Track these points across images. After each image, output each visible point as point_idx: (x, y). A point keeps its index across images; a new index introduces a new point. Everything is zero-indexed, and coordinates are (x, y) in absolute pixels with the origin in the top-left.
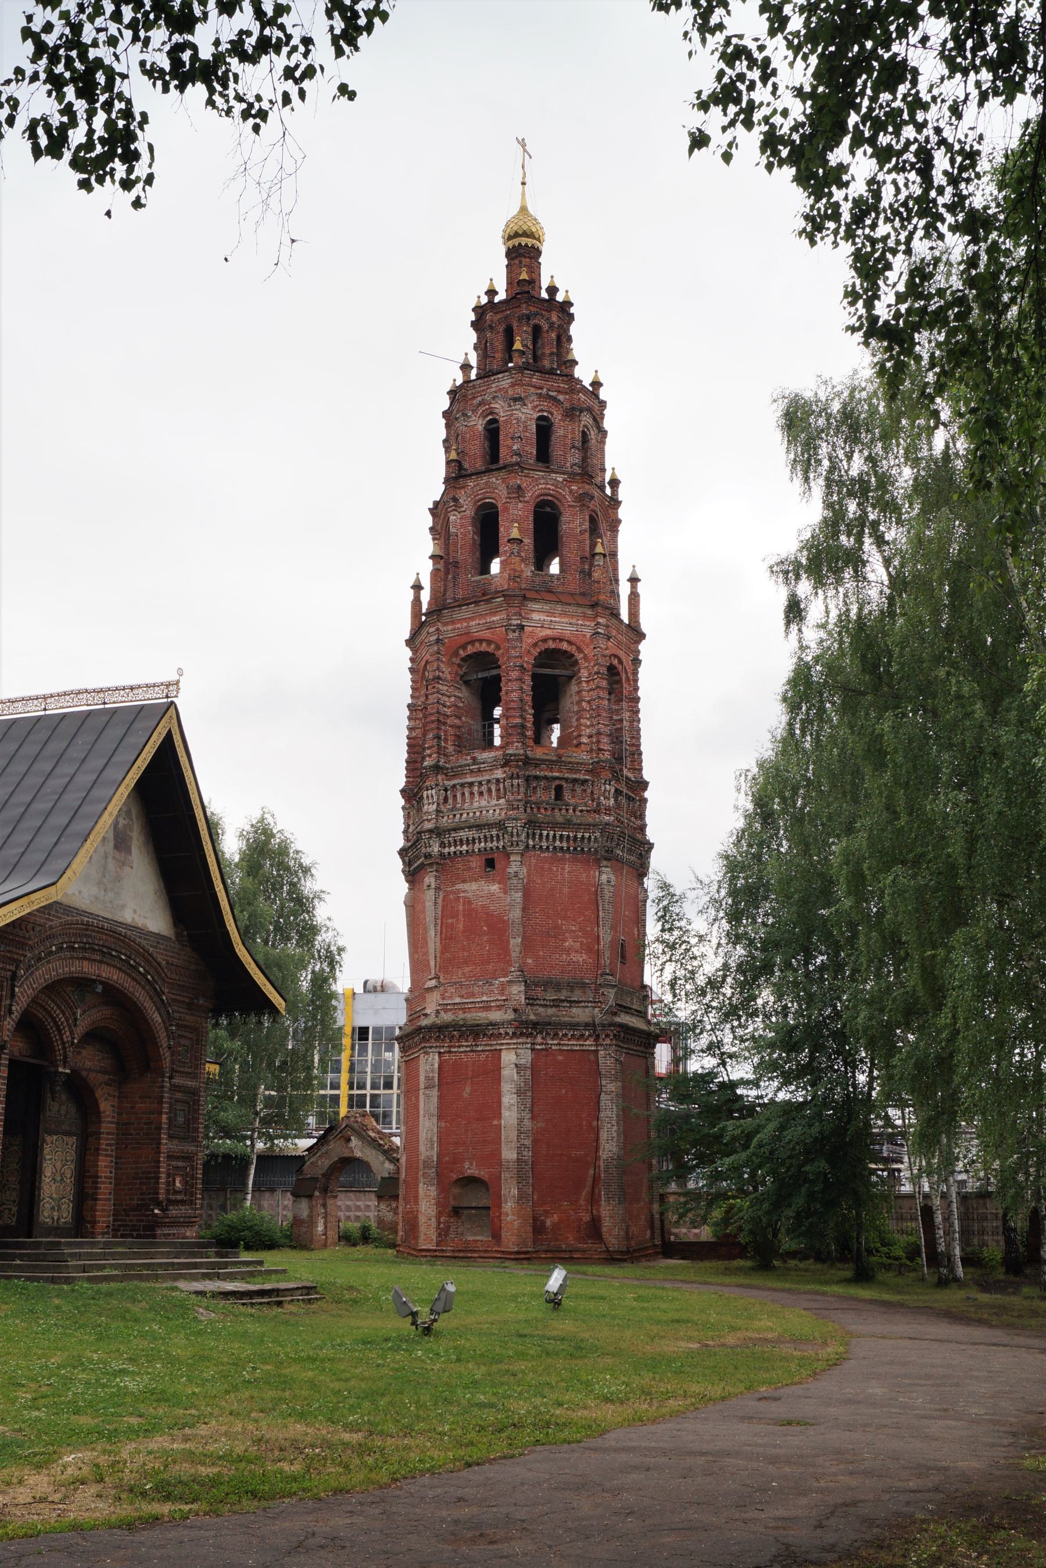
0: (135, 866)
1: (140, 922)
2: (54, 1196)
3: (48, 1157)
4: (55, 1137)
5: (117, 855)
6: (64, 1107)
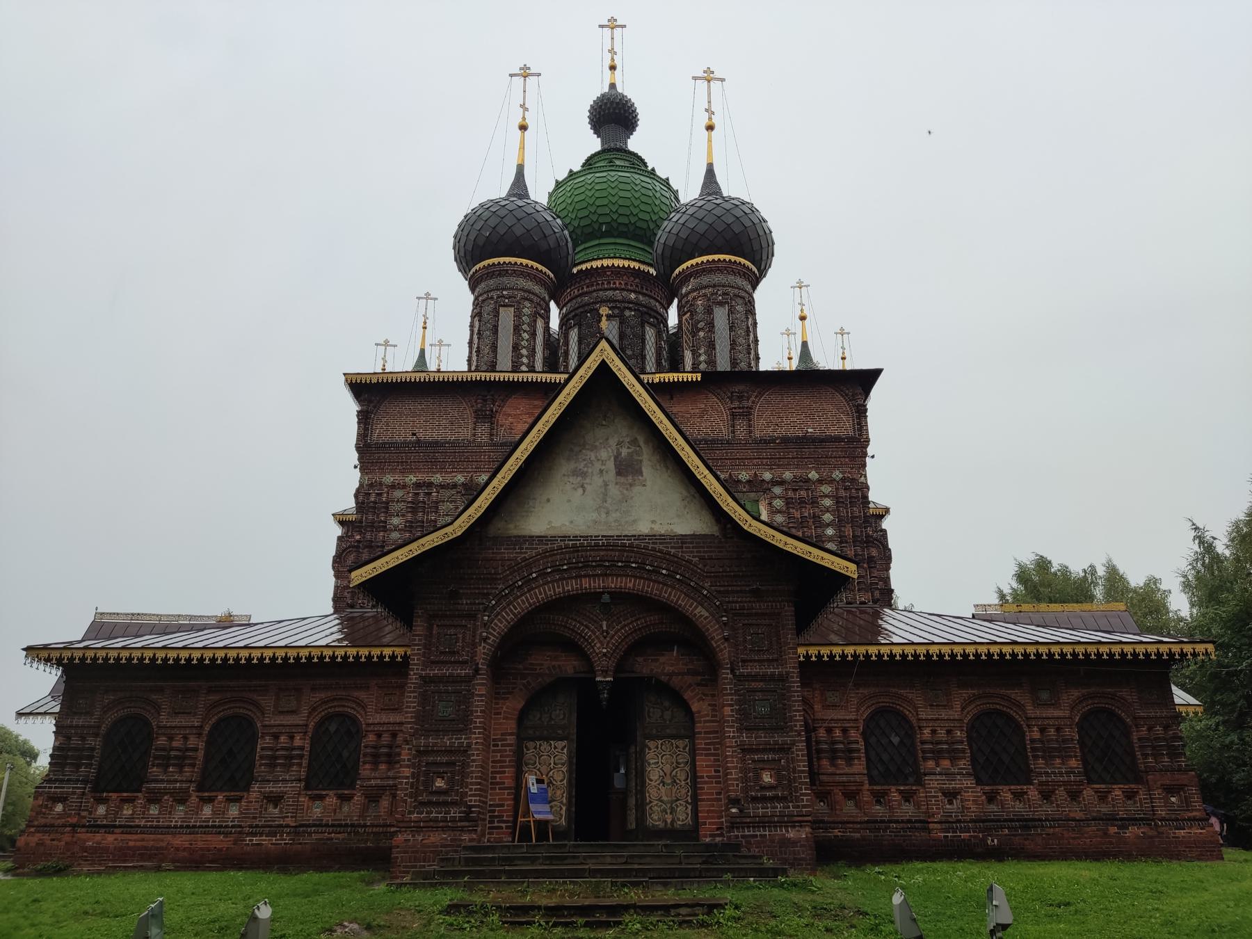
0: (648, 483)
1: (660, 529)
2: (665, 798)
4: (660, 742)
5: (622, 480)
6: (669, 713)
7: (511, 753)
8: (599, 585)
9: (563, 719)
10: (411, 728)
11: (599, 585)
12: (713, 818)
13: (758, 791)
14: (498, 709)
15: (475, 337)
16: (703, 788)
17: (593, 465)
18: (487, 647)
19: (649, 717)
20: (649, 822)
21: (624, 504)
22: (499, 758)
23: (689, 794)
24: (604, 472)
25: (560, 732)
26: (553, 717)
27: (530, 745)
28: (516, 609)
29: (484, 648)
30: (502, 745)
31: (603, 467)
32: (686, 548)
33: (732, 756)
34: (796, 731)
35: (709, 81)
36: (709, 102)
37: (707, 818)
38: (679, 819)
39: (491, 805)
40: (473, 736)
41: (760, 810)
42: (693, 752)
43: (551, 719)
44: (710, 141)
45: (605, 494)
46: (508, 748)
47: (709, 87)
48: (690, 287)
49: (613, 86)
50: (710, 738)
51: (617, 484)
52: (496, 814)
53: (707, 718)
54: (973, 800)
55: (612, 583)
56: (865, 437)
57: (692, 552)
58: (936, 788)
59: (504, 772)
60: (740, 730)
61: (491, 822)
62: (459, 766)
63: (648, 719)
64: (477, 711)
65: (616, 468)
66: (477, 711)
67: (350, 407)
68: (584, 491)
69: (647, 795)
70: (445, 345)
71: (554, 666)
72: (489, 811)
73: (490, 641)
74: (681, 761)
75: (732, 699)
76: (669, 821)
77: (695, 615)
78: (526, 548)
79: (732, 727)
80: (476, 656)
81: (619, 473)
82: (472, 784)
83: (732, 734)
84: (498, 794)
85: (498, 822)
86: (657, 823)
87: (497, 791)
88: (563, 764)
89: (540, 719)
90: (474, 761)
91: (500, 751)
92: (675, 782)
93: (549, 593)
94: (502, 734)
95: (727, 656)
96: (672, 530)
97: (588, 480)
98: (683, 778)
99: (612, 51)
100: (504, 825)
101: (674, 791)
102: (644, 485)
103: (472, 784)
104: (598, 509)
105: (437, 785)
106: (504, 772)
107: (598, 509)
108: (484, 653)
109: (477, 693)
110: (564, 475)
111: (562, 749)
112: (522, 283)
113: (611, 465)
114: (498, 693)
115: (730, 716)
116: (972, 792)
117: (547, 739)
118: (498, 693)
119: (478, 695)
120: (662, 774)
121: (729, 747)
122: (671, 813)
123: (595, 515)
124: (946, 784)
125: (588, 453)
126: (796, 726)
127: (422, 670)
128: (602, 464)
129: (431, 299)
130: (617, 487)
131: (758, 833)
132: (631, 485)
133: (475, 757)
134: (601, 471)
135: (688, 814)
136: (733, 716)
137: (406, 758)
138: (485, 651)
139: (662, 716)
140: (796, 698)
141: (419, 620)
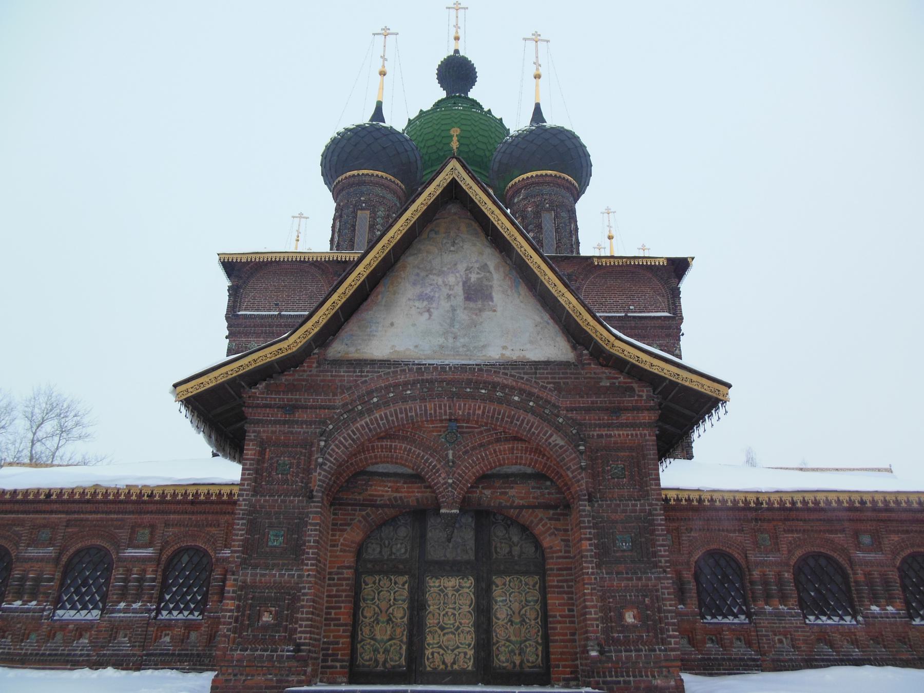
0: (499, 309)
2: (513, 638)
3: (499, 599)
4: (508, 579)
5: (472, 305)
7: (348, 588)
8: (445, 411)
9: (405, 553)
10: (238, 557)
11: (445, 411)
12: (566, 660)
13: (619, 632)
14: (335, 540)
15: (336, 235)
16: (555, 629)
17: (440, 289)
18: (323, 473)
19: (496, 553)
20: (496, 663)
21: (473, 329)
22: (334, 593)
23: (540, 634)
24: (452, 297)
25: (401, 566)
26: (394, 550)
27: (369, 579)
28: (355, 434)
29: (320, 474)
30: (339, 579)
31: (451, 292)
32: (540, 374)
33: (591, 594)
34: (661, 567)
35: (536, 42)
36: (537, 57)
37: (560, 660)
38: (528, 661)
39: (324, 643)
40: (305, 567)
41: (623, 654)
42: (544, 591)
43: (391, 553)
44: (537, 85)
45: (453, 320)
46: (344, 583)
47: (537, 46)
48: (521, 197)
49: (457, 51)
50: (562, 575)
51: (465, 309)
52: (330, 652)
53: (560, 554)
54: (803, 640)
55: (460, 409)
56: (679, 315)
57: (547, 378)
58: (767, 627)
59: (340, 608)
60: (598, 566)
61: (324, 661)
62: (289, 599)
63: (495, 556)
64: (309, 541)
65: (464, 293)
66: (309, 541)
67: (224, 282)
68: (430, 315)
69: (494, 634)
70: (304, 218)
71: (395, 498)
72: (323, 649)
73: (326, 467)
74: (530, 599)
75: (590, 533)
76: (518, 662)
77: (550, 444)
78: (367, 372)
79: (591, 562)
80: (311, 483)
81: (468, 298)
82: (302, 620)
83: (590, 571)
84: (333, 631)
85: (332, 661)
86: (505, 665)
87: (332, 627)
88: (404, 601)
89: (381, 552)
90: (304, 594)
91: (335, 585)
92: (524, 620)
93: (390, 419)
94: (338, 568)
95: (584, 487)
96: (524, 356)
97: (434, 305)
98: (533, 617)
99: (457, 27)
100: (338, 664)
101: (523, 630)
102: (495, 311)
103: (302, 620)
104: (445, 334)
105: (264, 619)
106: (340, 608)
107: (445, 334)
108: (320, 480)
109: (310, 521)
110: (409, 299)
111: (403, 585)
112: (378, 190)
113: (459, 290)
114: (336, 524)
115: (587, 551)
116: (802, 632)
117: (386, 573)
118: (336, 524)
119: (311, 524)
120: (510, 612)
121: (587, 584)
122: (520, 654)
123: (441, 340)
124: (776, 623)
125: (435, 277)
126: (660, 561)
127: (253, 496)
128: (450, 289)
129: (304, 218)
130: (466, 312)
131: (622, 679)
132: (480, 310)
133: (306, 591)
134: (449, 296)
135: (537, 655)
136: (592, 550)
137: (231, 589)
138: (321, 477)
139: (510, 552)
140: (660, 532)
141: (251, 443)
